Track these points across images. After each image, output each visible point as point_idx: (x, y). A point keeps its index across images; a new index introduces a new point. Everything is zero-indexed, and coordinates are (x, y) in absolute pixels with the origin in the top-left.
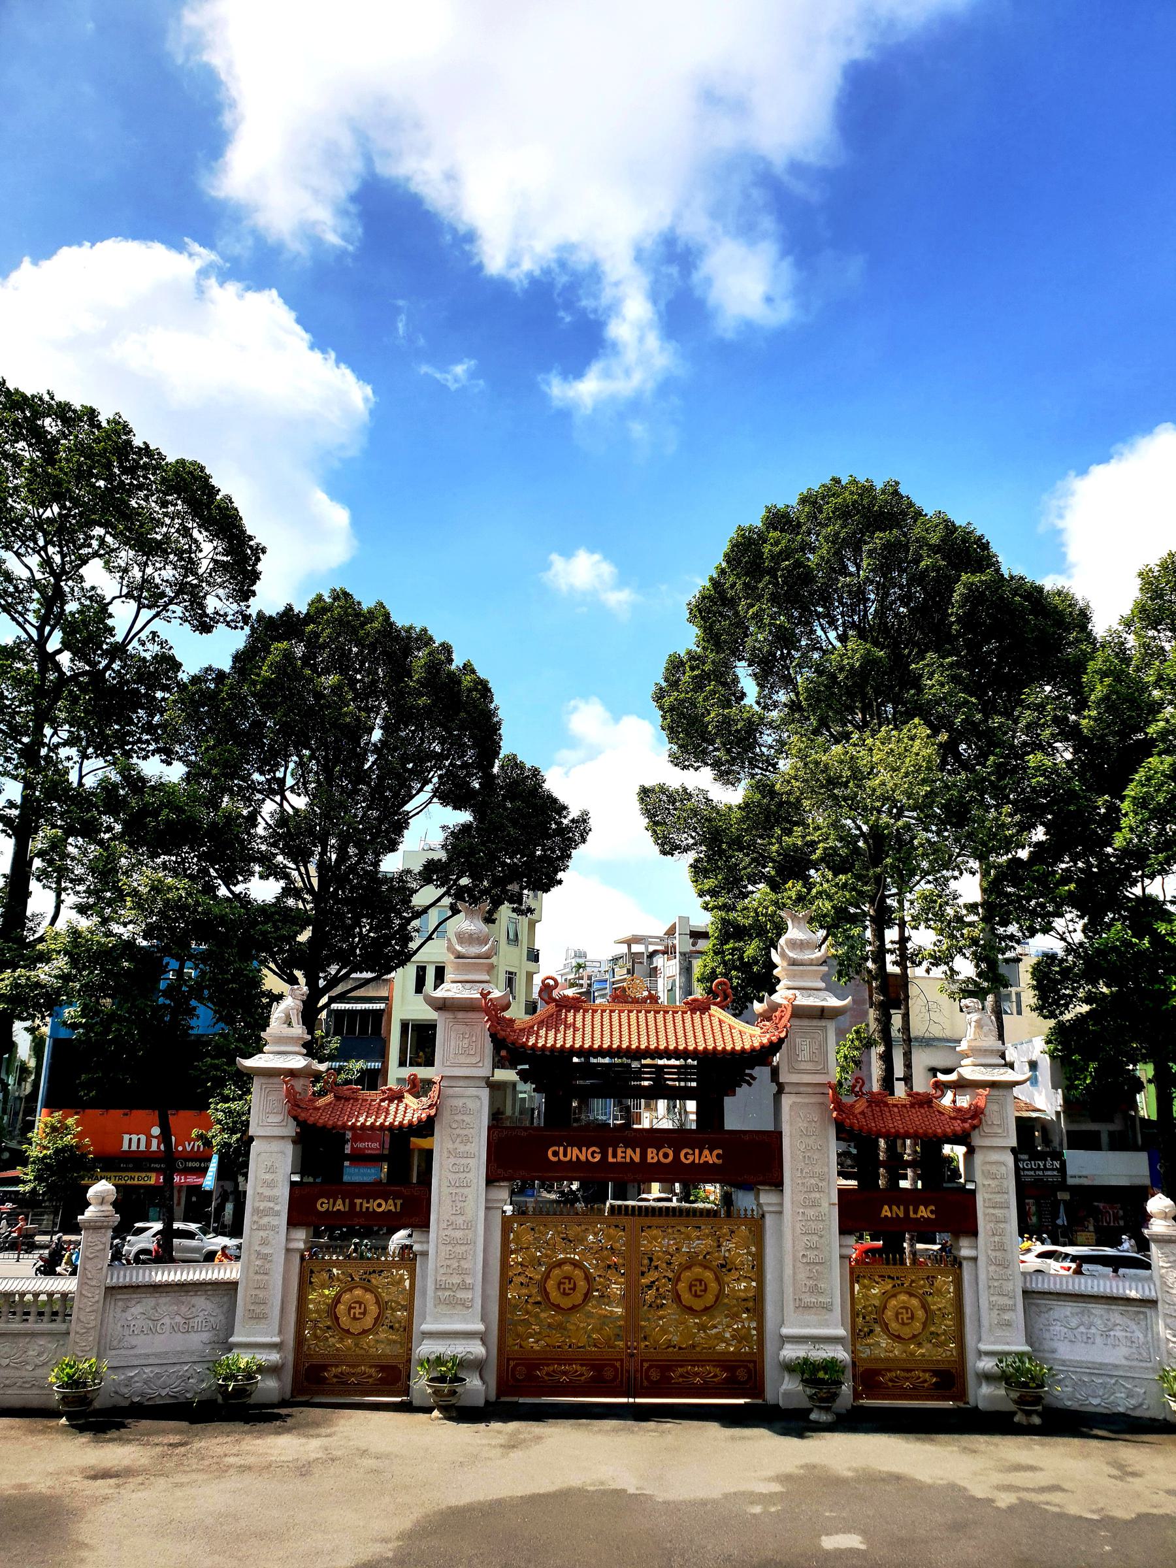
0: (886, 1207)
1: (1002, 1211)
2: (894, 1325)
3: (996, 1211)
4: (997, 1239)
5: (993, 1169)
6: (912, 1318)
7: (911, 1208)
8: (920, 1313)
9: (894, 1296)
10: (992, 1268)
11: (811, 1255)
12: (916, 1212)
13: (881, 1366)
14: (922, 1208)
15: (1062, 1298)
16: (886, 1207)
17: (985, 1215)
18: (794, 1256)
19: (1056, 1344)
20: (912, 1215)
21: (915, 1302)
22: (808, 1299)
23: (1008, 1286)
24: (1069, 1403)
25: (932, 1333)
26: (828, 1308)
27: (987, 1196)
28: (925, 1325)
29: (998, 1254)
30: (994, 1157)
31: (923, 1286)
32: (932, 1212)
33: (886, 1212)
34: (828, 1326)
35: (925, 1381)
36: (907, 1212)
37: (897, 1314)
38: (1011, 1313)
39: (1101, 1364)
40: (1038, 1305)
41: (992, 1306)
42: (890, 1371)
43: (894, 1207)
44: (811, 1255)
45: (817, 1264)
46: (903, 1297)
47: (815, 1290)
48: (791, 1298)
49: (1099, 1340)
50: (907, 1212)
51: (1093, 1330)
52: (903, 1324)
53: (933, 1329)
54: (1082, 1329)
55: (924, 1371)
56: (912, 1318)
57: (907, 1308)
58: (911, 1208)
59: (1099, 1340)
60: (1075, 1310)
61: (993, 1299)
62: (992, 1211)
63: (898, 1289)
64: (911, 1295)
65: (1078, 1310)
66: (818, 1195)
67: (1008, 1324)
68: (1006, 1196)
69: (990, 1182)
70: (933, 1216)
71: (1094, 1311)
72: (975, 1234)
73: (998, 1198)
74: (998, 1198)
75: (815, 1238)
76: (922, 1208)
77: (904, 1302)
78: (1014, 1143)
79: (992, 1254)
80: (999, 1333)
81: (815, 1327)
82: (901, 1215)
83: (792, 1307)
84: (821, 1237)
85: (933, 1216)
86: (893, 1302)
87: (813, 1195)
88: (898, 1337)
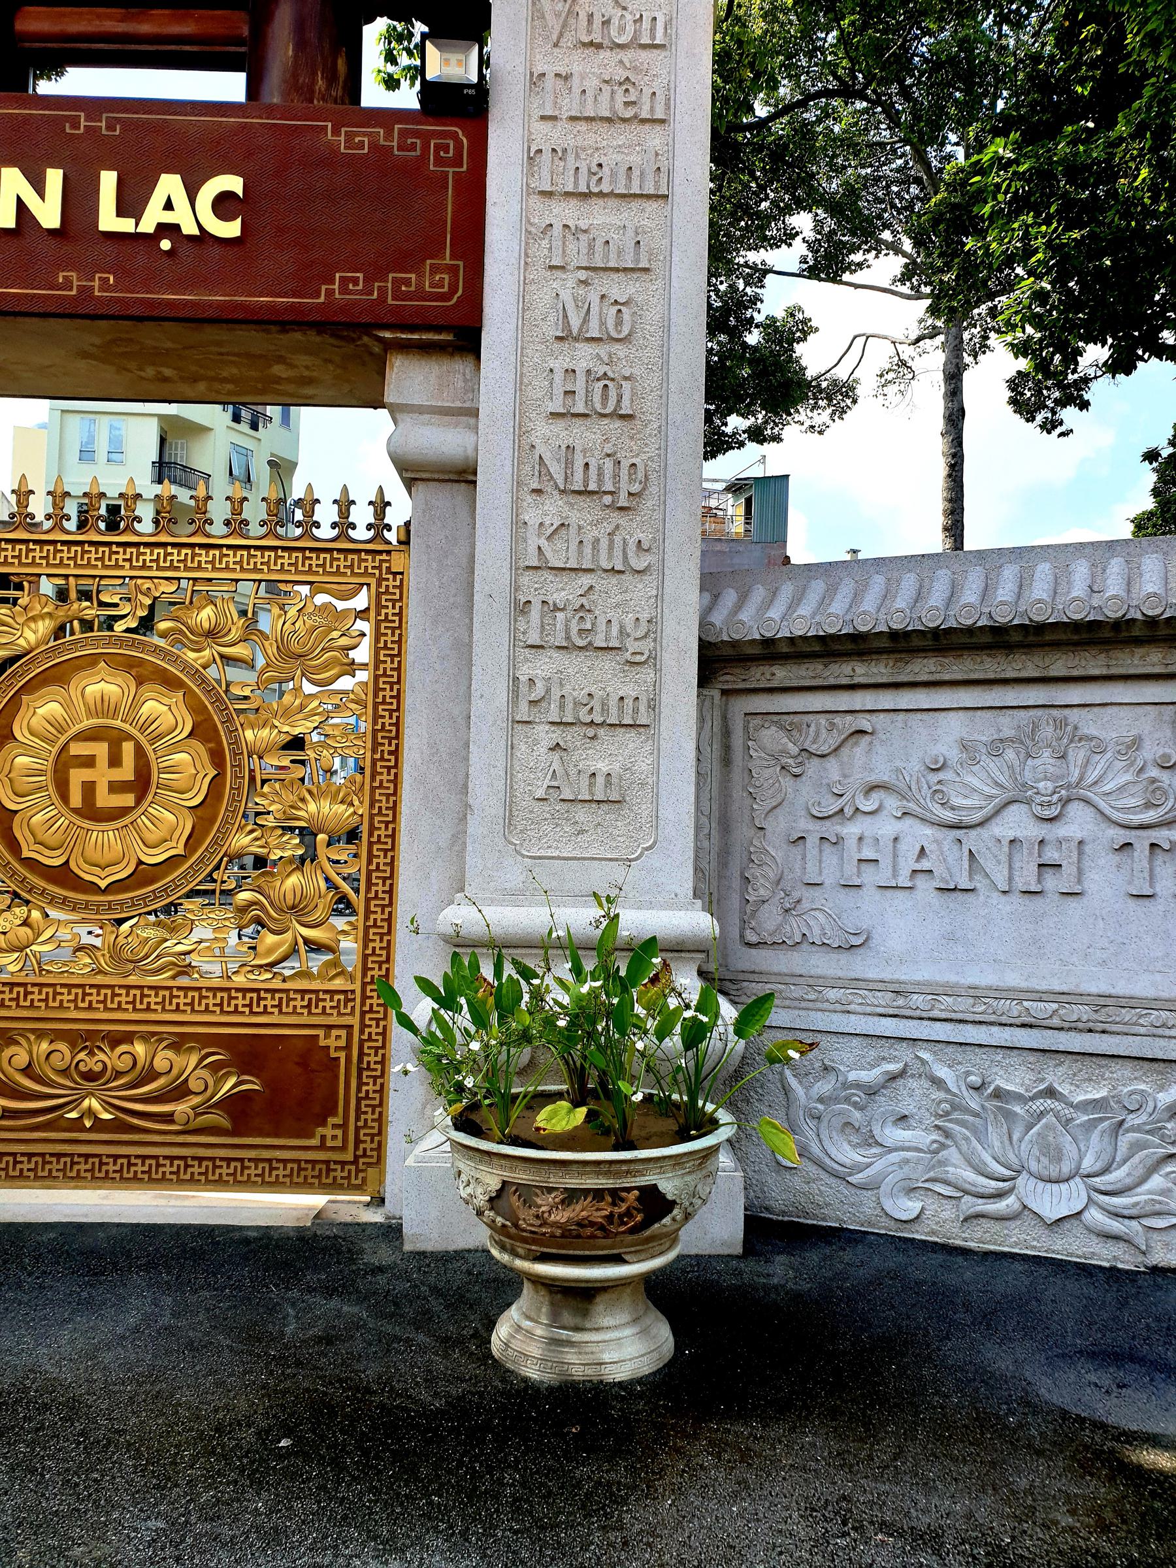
3: (600, 217)
4: (584, 357)
6: (141, 784)
7: (108, 181)
8: (185, 767)
10: (552, 509)
12: (129, 205)
14: (170, 185)
15: (923, 668)
17: (533, 233)
19: (867, 910)
20: (109, 220)
24: (908, 1208)
27: (547, 136)
28: (204, 813)
31: (212, 634)
32: (224, 205)
35: (180, 1092)
36: (79, 199)
37: (63, 765)
38: (630, 738)
39: (1102, 1002)
40: (787, 721)
41: (526, 706)
49: (1105, 879)
50: (79, 199)
51: (1078, 823)
52: (91, 812)
53: (241, 841)
54: (1018, 823)
55: (178, 1044)
56: (141, 784)
57: (115, 739)
58: (108, 181)
59: (1105, 879)
60: (984, 729)
61: (541, 667)
62: (565, 212)
63: (79, 644)
64: (144, 675)
65: (1007, 724)
68: (654, 138)
69: (577, 63)
70: (231, 229)
71: (1089, 724)
72: (464, 339)
73: (618, 150)
74: (618, 150)
76: (170, 185)
77: (103, 707)
79: (547, 436)
82: (49, 214)
85: (231, 229)
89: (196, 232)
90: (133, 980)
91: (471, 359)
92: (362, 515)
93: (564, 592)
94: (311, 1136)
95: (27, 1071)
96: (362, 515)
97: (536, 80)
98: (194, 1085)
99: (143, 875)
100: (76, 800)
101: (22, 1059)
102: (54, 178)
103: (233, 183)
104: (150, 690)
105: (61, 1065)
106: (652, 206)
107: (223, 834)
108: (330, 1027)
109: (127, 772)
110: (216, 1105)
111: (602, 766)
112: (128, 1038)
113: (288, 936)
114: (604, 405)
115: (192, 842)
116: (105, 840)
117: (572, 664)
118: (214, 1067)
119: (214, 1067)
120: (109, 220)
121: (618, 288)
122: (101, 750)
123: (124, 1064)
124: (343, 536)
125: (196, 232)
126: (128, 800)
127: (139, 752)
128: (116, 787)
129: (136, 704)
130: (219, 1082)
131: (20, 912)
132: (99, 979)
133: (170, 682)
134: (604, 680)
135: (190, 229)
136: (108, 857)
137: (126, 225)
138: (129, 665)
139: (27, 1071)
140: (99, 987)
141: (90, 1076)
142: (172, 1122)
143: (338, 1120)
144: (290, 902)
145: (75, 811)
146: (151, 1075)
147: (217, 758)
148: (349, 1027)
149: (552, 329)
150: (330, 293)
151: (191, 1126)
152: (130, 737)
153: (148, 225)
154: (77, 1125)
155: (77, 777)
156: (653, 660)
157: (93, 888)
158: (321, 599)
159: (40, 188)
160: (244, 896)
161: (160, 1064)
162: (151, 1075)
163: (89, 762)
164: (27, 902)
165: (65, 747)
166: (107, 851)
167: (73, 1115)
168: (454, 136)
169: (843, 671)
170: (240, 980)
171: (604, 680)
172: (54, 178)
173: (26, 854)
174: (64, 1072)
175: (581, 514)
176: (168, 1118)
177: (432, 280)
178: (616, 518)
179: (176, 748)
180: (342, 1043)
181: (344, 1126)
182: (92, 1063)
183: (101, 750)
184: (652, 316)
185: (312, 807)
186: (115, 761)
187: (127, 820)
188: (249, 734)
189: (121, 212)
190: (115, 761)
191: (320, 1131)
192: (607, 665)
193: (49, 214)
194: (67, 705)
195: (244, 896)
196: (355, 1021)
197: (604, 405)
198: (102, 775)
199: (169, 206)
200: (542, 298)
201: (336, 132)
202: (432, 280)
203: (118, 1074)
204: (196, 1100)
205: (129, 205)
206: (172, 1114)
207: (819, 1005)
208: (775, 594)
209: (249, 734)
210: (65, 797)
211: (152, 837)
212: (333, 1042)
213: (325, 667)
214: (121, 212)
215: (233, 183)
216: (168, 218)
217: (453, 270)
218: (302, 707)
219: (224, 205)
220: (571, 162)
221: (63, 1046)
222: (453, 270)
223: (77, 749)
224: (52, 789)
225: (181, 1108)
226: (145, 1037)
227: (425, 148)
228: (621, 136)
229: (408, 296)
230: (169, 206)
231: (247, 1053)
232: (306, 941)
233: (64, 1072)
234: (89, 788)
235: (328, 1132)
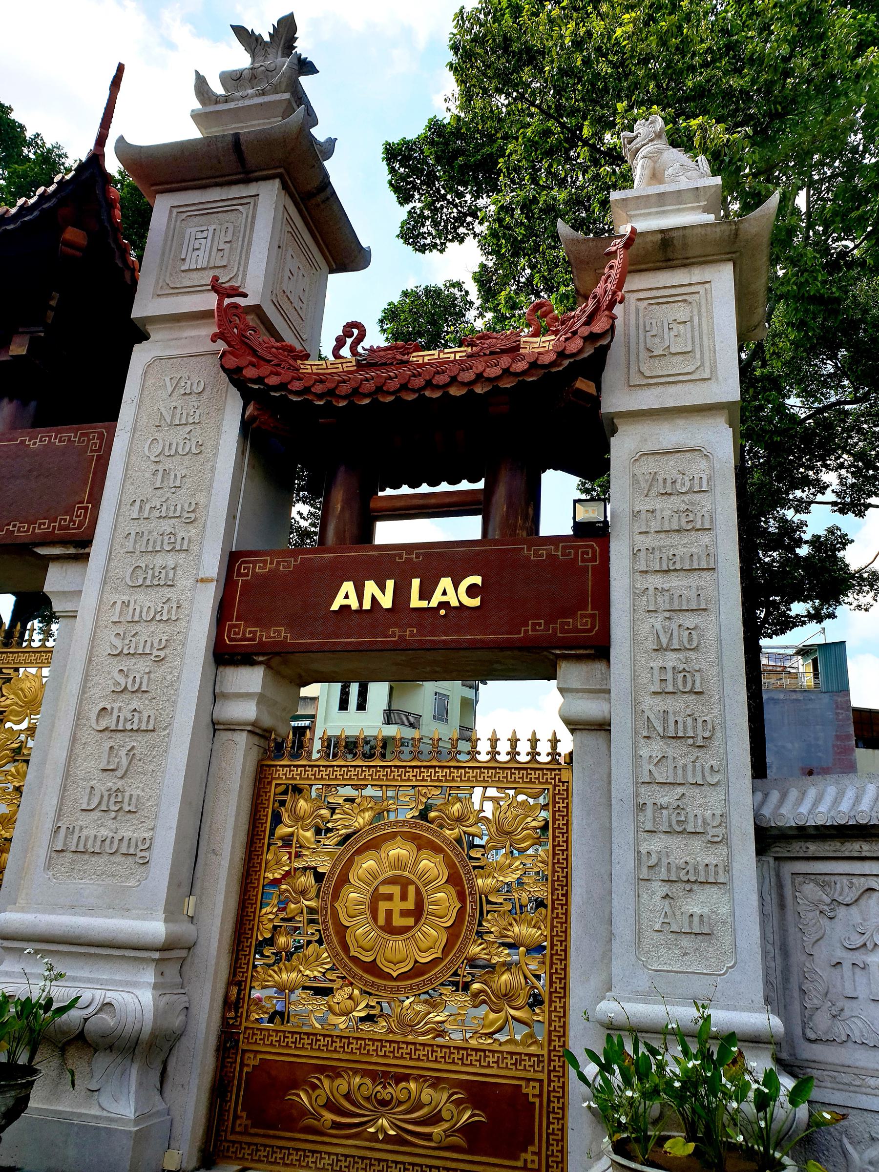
0: (348, 587)
1: (693, 580)
2: (362, 931)
3: (675, 582)
4: (671, 660)
5: (669, 468)
6: (418, 912)
7: (416, 583)
8: (443, 900)
9: (373, 845)
10: (656, 748)
11: (124, 706)
12: (426, 594)
13: (307, 1055)
14: (446, 583)
16: (348, 587)
17: (636, 594)
18: (79, 715)
20: (415, 602)
21: (430, 865)
22: (95, 828)
23: (704, 806)
25: (472, 962)
26: (138, 855)
28: (453, 932)
29: (676, 705)
30: (670, 435)
32: (472, 591)
33: (346, 595)
34: (125, 911)
35: (435, 1119)
36: (402, 594)
37: (376, 898)
40: (823, 881)
41: (647, 869)
42: (335, 1073)
43: (370, 587)
44: (124, 706)
45: (127, 732)
46: (398, 851)
47: (117, 806)
48: (48, 825)
50: (402, 594)
52: (391, 929)
53: (475, 950)
55: (436, 1083)
56: (418, 912)
57: (404, 883)
58: (416, 583)
61: (655, 845)
62: (657, 581)
64: (421, 844)
66: (170, 560)
67: (703, 933)
68: (705, 539)
69: (658, 504)
70: (476, 602)
74: (684, 547)
75: (141, 666)
76: (446, 583)
77: (399, 864)
78: (729, 389)
79: (651, 705)
80: (667, 960)
81: (90, 910)
82: (386, 601)
83: (41, 853)
84: (160, 661)
85: (476, 602)
86: (368, 864)
87: (159, 561)
88: (372, 968)
89: (457, 604)
90: (410, 1038)
91: (604, 663)
92: (544, 748)
93: (666, 797)
94: (517, 1158)
95: (347, 1096)
96: (544, 748)
97: (636, 514)
98: (445, 1115)
99: (418, 970)
100: (381, 921)
101: (344, 1088)
102: (390, 584)
103: (477, 580)
104: (425, 853)
105: (366, 1093)
106: (706, 574)
107: (465, 945)
108: (528, 1080)
109: (410, 905)
110: (459, 1130)
111: (697, 910)
112: (406, 1078)
113: (502, 1014)
114: (685, 686)
115: (446, 950)
116: (397, 946)
117: (674, 843)
118: (458, 1103)
119: (458, 1103)
120: (415, 602)
121: (689, 621)
122: (396, 890)
123: (403, 1096)
124: (533, 760)
125: (457, 604)
126: (410, 921)
127: (418, 892)
128: (404, 913)
129: (416, 863)
130: (461, 1113)
131: (348, 990)
132: (391, 1037)
133: (437, 849)
134: (696, 854)
135: (454, 603)
136: (398, 957)
137: (424, 604)
138: (414, 838)
139: (347, 1096)
140: (390, 1042)
141: (384, 1103)
142: (431, 1140)
143: (535, 1149)
144: (503, 992)
145: (381, 928)
146: (419, 1106)
147: (461, 896)
148: (541, 1081)
149: (651, 645)
150: (526, 631)
151: (443, 1144)
152: (412, 882)
153: (434, 603)
154: (373, 1137)
155: (383, 906)
156: (725, 841)
157: (389, 977)
158: (521, 798)
159: (383, 590)
160: (476, 986)
161: (425, 1098)
162: (419, 1106)
163: (389, 897)
164: (351, 984)
165: (377, 889)
166: (398, 954)
167: (372, 1130)
168: (592, 547)
169: (855, 847)
170: (473, 1042)
171: (696, 854)
172: (390, 584)
173: (352, 953)
174: (368, 1099)
175: (673, 750)
176: (428, 1137)
177: (582, 622)
178: (697, 753)
179: (438, 890)
180: (537, 1092)
181: (538, 1154)
182: (385, 1095)
183: (396, 890)
184: (710, 635)
185: (516, 929)
186: (404, 897)
187: (409, 934)
188: (480, 881)
189: (421, 598)
190: (404, 897)
191: (523, 1156)
192: (697, 843)
193: (386, 601)
194: (379, 862)
195: (476, 986)
196: (544, 1077)
197: (685, 686)
198: (397, 906)
199: (444, 593)
200: (644, 628)
201: (529, 550)
202: (582, 622)
203: (400, 1103)
204: (446, 1126)
205: (426, 594)
206: (431, 1134)
207: (864, 1090)
208: (804, 794)
209: (480, 881)
210: (375, 918)
211: (423, 946)
212: (531, 1090)
213: (523, 840)
214: (421, 598)
215: (477, 580)
216: (444, 599)
217: (593, 616)
218: (510, 865)
219: (472, 591)
220: (657, 554)
221: (368, 1081)
222: (593, 616)
223: (384, 889)
224: (368, 915)
225: (436, 1131)
226: (417, 1078)
227: (576, 554)
228: (686, 538)
229: (568, 631)
230: (444, 593)
231: (477, 1093)
232: (513, 1018)
233: (368, 1099)
234: (389, 914)
235: (529, 1157)
